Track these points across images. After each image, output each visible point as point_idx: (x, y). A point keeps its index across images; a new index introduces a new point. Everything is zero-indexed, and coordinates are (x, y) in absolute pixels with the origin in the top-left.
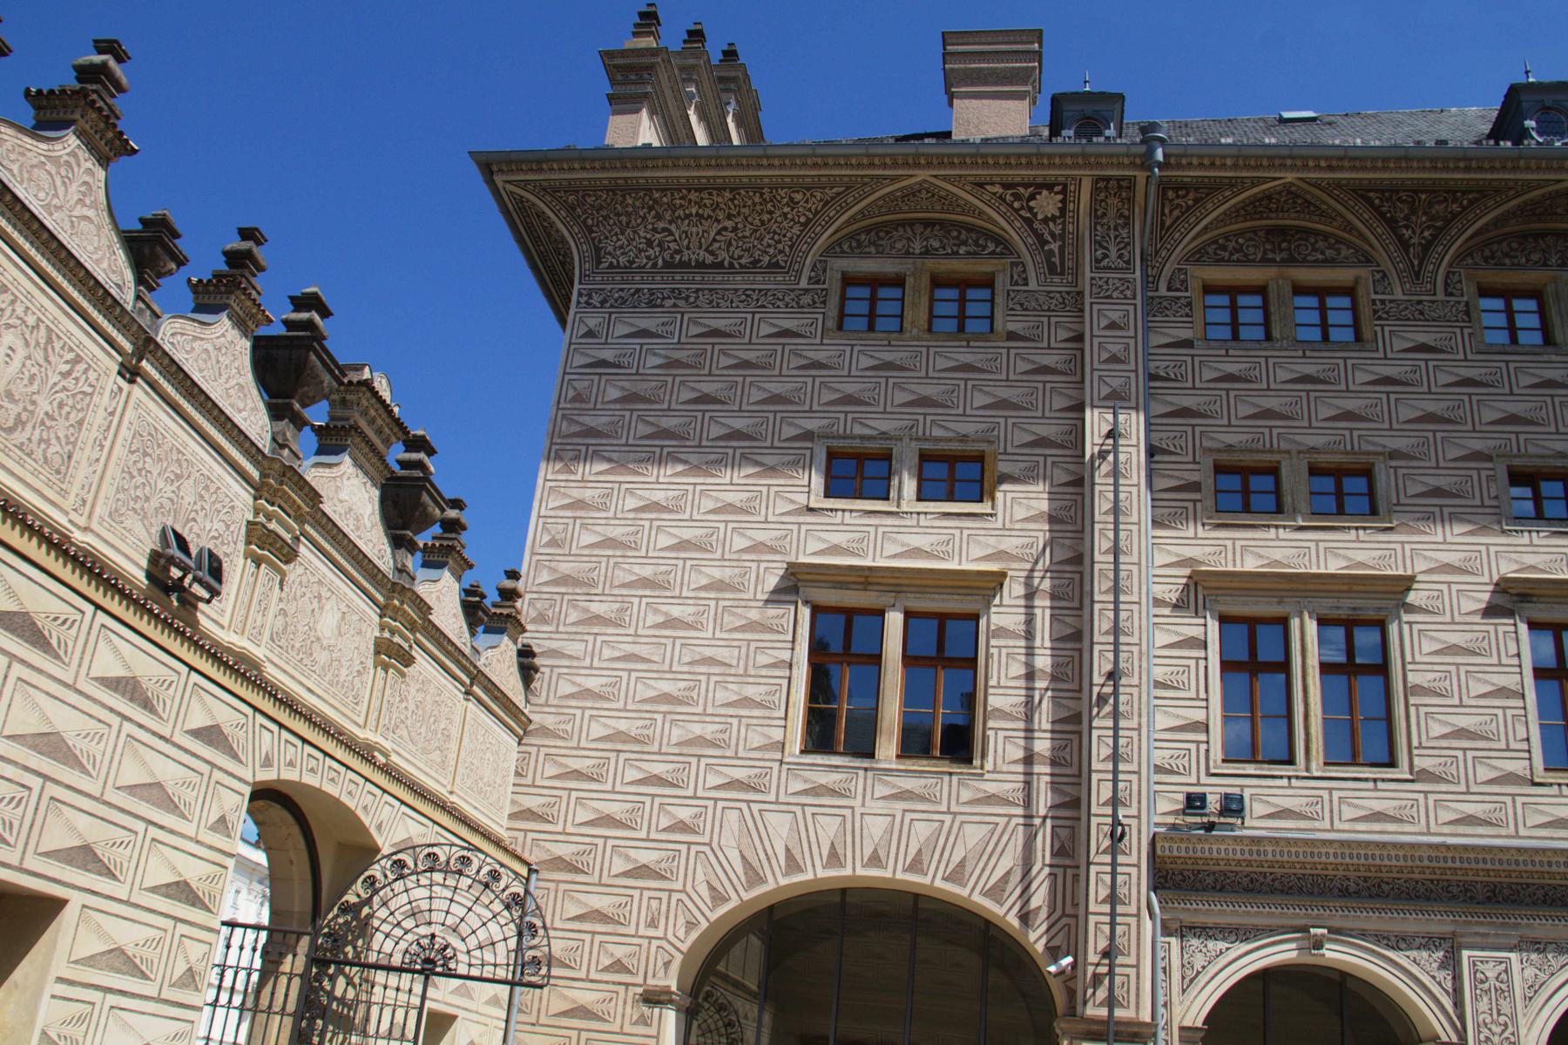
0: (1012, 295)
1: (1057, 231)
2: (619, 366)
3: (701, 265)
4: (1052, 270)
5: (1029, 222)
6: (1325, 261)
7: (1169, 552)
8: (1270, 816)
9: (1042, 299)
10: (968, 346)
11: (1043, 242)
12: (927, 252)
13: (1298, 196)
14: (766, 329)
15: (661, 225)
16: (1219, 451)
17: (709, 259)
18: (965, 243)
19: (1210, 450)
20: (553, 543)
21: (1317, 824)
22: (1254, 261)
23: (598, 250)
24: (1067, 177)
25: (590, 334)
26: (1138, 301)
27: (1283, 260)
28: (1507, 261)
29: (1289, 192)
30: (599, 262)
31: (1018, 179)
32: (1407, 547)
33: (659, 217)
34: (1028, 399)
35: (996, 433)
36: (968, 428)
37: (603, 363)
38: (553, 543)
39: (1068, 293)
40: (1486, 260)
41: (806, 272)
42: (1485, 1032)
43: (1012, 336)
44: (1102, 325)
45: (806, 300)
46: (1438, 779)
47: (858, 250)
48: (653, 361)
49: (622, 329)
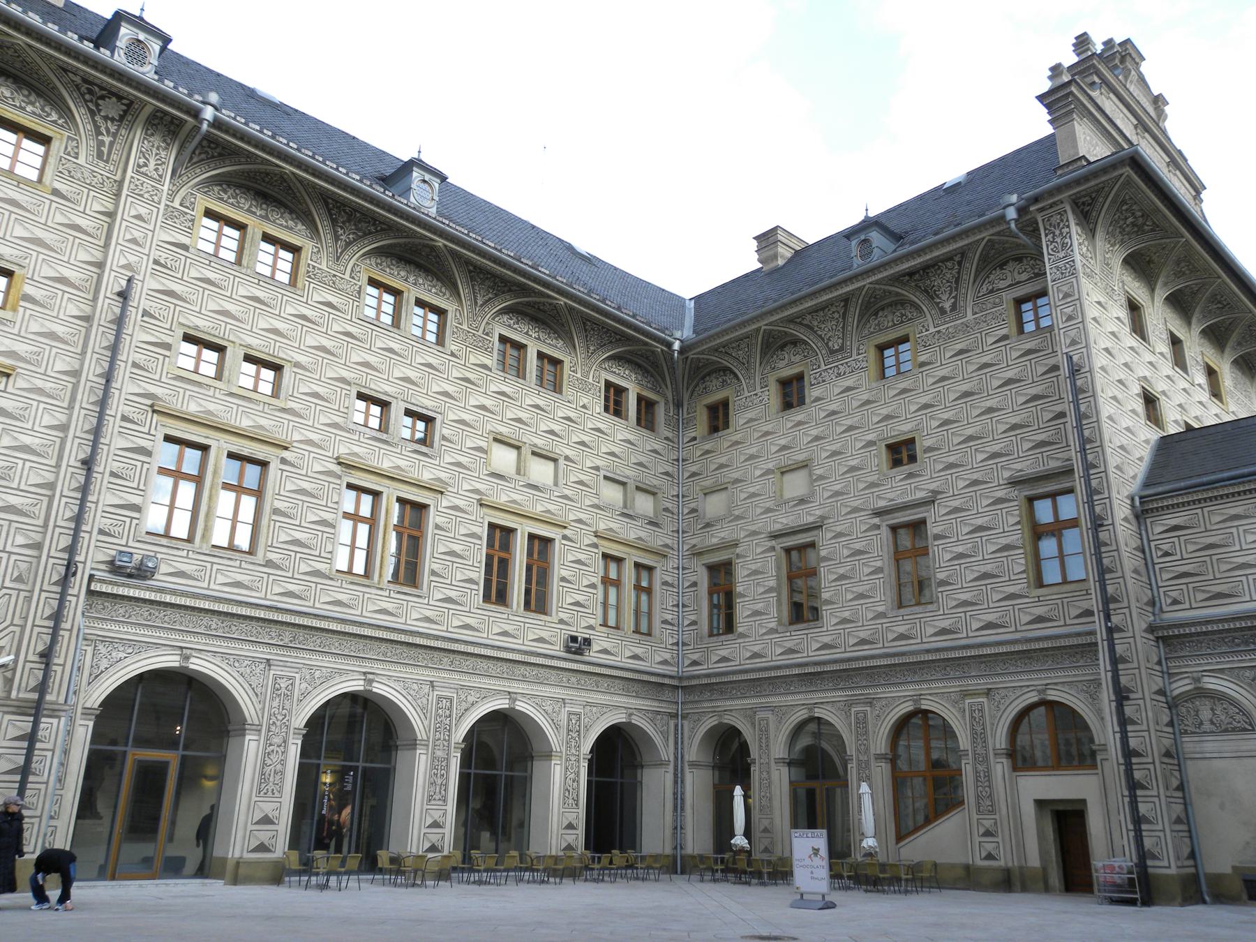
0: (64, 161)
1: (113, 130)
4: (100, 155)
6: (287, 227)
7: (139, 385)
8: (170, 574)
9: (86, 174)
10: (18, 187)
11: (99, 133)
13: (285, 181)
16: (189, 327)
18: (32, 104)
19: (183, 325)
21: (198, 584)
22: (242, 208)
24: (137, 97)
26: (162, 207)
27: (261, 216)
28: (388, 270)
29: (282, 177)
31: (98, 82)
32: (291, 423)
34: (59, 245)
35: (27, 261)
39: (108, 178)
40: (377, 264)
42: (274, 719)
43: (55, 192)
44: (132, 214)
46: (278, 567)
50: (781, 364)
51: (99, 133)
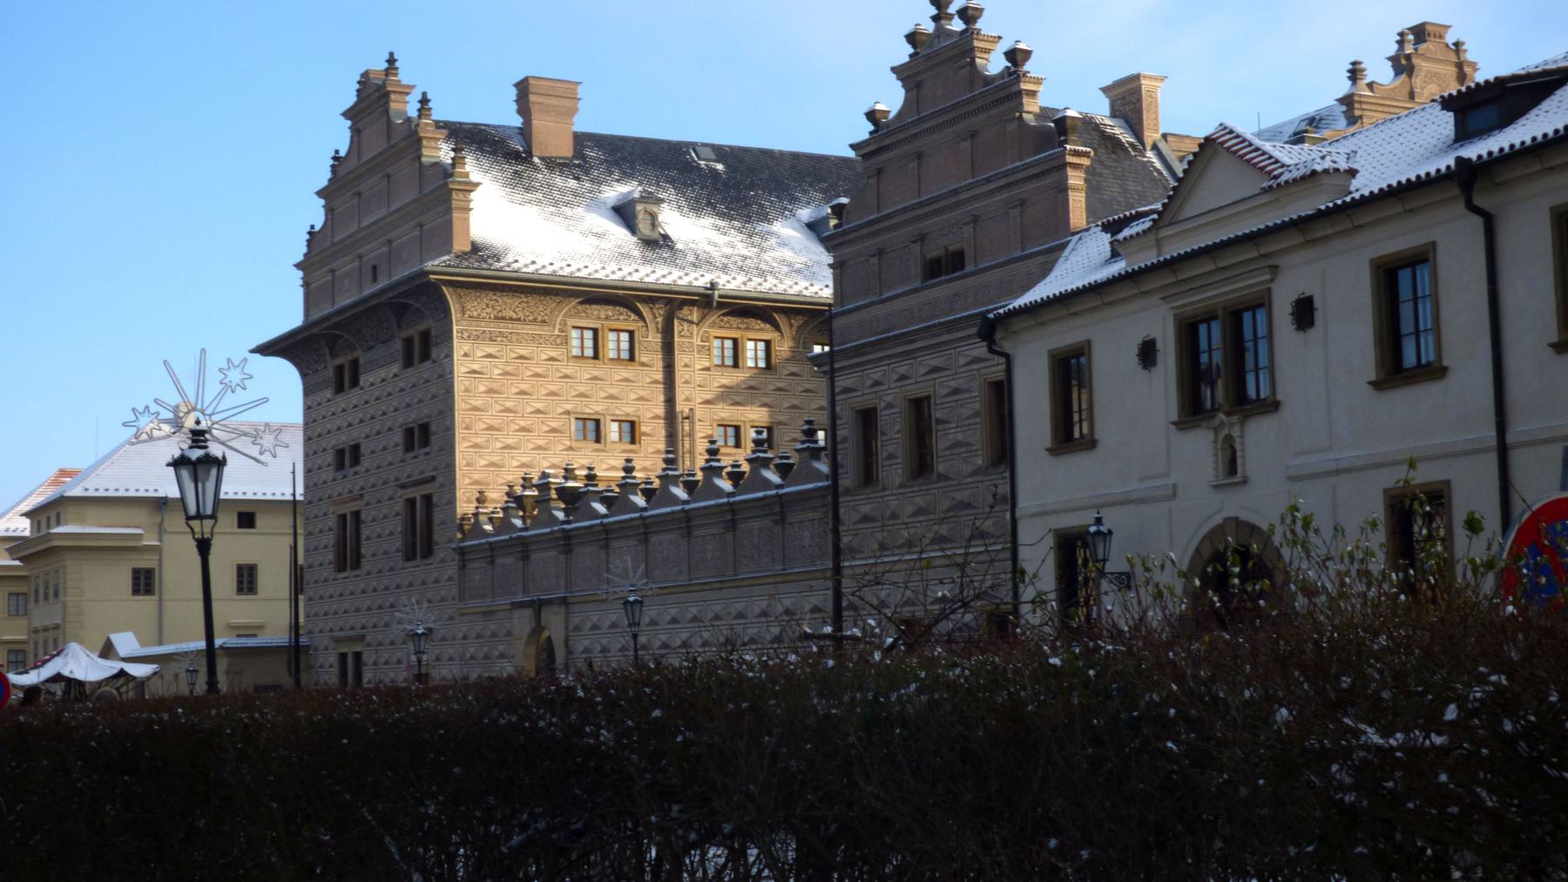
3: (511, 319)
5: (651, 308)
12: (607, 318)
14: (544, 357)
17: (515, 316)
18: (622, 314)
20: (468, 465)
23: (463, 307)
25: (466, 355)
30: (464, 314)
33: (494, 294)
36: (629, 410)
37: (474, 372)
38: (468, 465)
41: (558, 326)
43: (643, 364)
45: (559, 341)
47: (578, 315)
48: (497, 371)
49: (480, 354)
51: (655, 317)
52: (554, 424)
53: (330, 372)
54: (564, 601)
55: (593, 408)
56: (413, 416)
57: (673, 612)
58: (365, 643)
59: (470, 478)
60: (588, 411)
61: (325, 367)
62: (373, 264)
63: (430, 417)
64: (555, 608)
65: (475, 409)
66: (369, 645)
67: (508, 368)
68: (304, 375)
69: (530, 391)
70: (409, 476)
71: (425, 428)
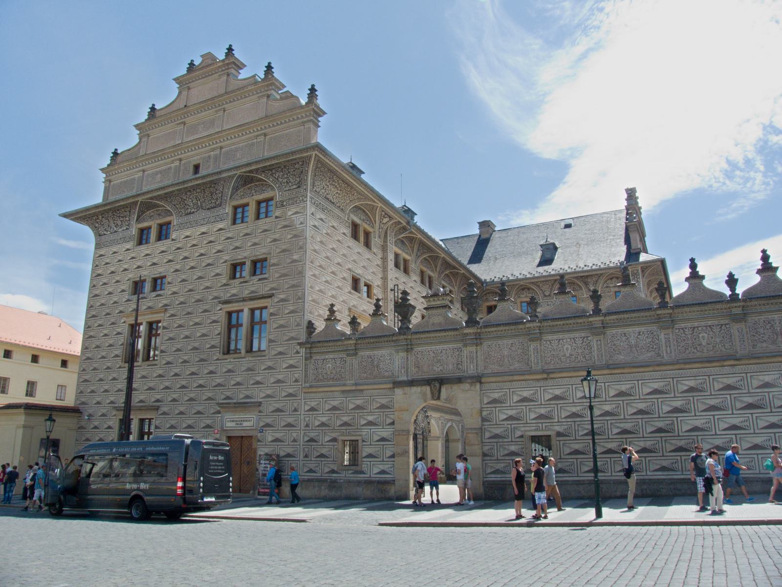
2: (318, 229)
3: (331, 201)
5: (380, 222)
15: (328, 184)
20: (311, 287)
25: (312, 214)
33: (329, 182)
36: (370, 278)
37: (315, 226)
38: (311, 287)
43: (374, 253)
48: (325, 232)
50: (523, 296)
52: (345, 275)
53: (134, 231)
54: (478, 379)
55: (359, 271)
56: (246, 254)
57: (655, 386)
58: (160, 412)
59: (312, 297)
60: (357, 272)
61: (127, 229)
62: (196, 163)
63: (270, 254)
64: (466, 386)
65: (315, 251)
66: (164, 413)
67: (329, 231)
68: (98, 235)
69: (336, 249)
70: (234, 295)
71: (258, 265)
